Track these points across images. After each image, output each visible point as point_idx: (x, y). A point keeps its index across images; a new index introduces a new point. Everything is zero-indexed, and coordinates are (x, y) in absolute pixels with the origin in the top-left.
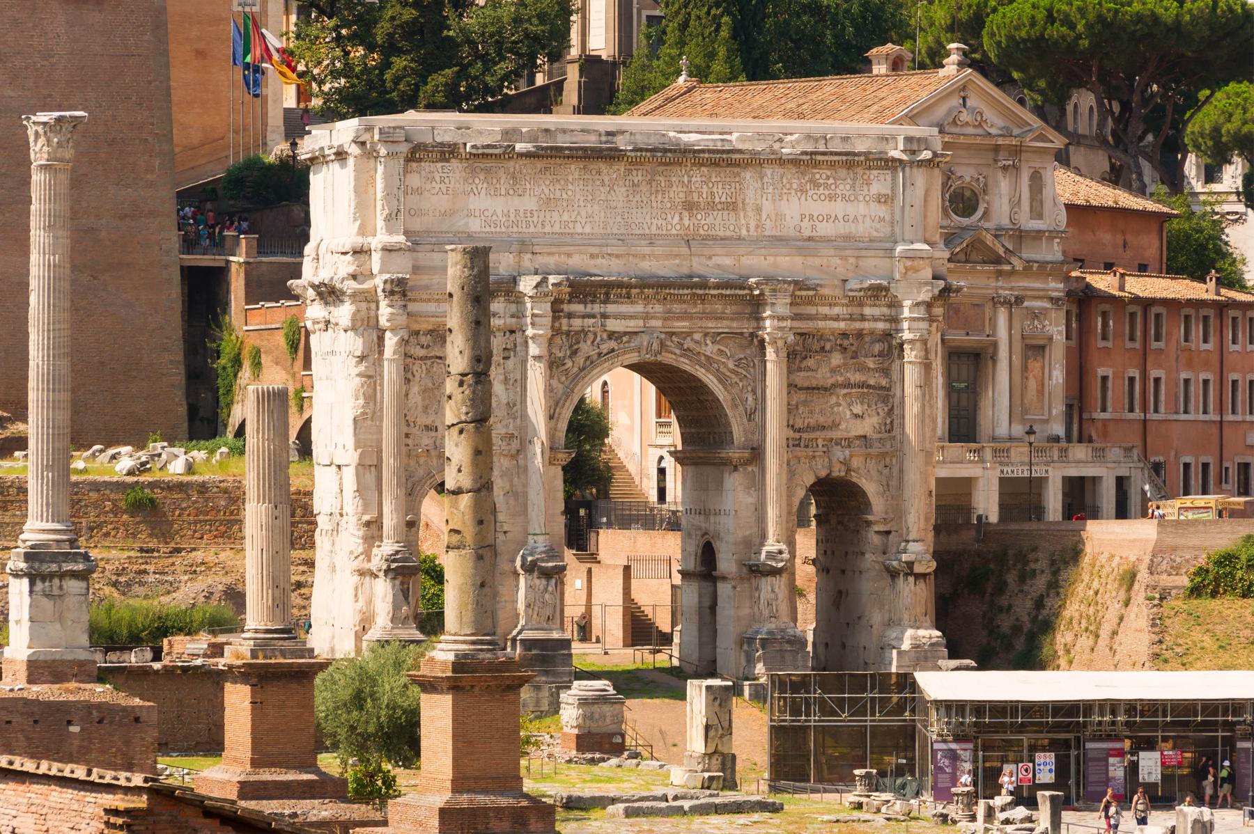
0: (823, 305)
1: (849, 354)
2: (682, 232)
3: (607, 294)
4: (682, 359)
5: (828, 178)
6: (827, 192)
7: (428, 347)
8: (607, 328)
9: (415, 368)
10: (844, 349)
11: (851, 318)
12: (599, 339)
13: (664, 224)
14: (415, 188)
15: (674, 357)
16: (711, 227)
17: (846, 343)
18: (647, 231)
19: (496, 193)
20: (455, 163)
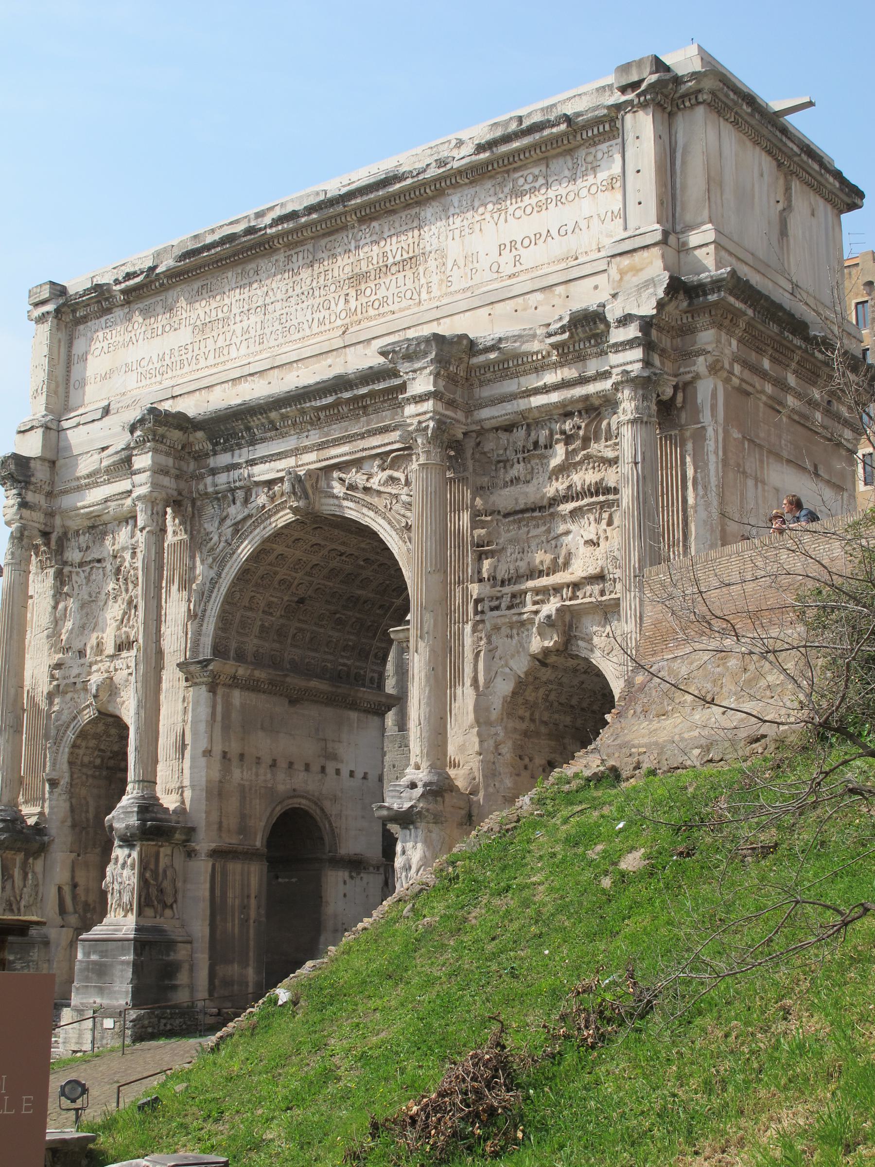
0: (526, 373)
1: (578, 443)
2: (348, 320)
3: (248, 429)
4: (346, 503)
5: (536, 178)
6: (534, 200)
7: (88, 548)
8: (256, 479)
9: (74, 577)
10: (568, 439)
12: (254, 496)
13: (327, 316)
14: (80, 355)
16: (384, 301)
17: (568, 426)
18: (308, 332)
19: (154, 335)
20: (119, 313)
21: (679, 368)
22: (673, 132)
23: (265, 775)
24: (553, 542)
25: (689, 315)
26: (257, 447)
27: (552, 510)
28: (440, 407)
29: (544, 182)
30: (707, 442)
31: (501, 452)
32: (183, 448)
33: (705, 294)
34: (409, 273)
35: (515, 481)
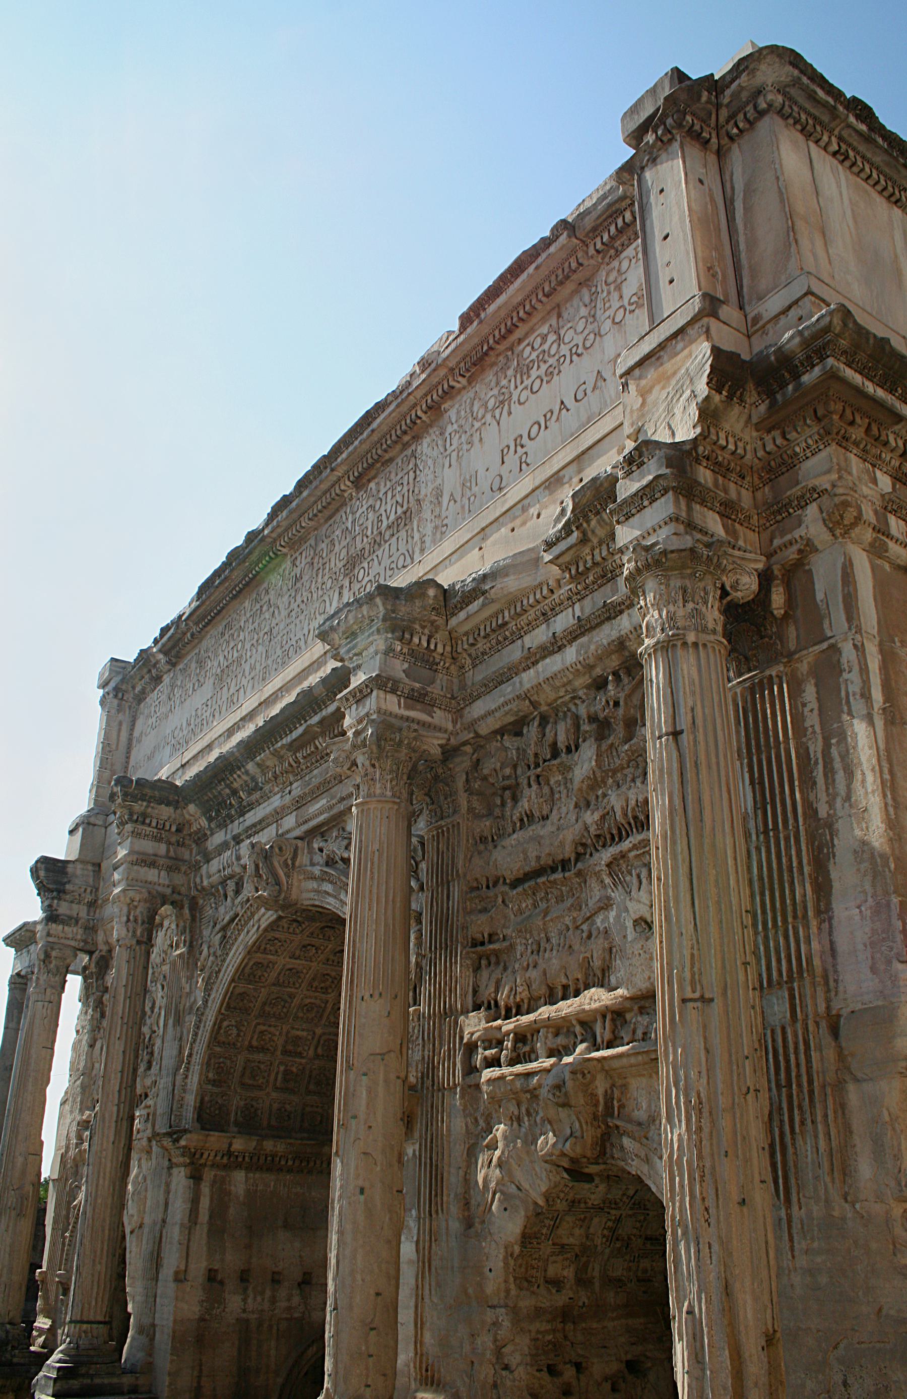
0: (531, 626)
5: (544, 338)
11: (583, 628)
15: (313, 885)
21: (771, 541)
22: (727, 177)
23: (289, 1300)
24: (585, 927)
25: (776, 433)
26: (247, 816)
27: (580, 865)
28: (392, 703)
29: (555, 337)
30: (845, 675)
31: (508, 771)
32: (179, 830)
33: (797, 376)
34: (403, 534)
35: (528, 819)
